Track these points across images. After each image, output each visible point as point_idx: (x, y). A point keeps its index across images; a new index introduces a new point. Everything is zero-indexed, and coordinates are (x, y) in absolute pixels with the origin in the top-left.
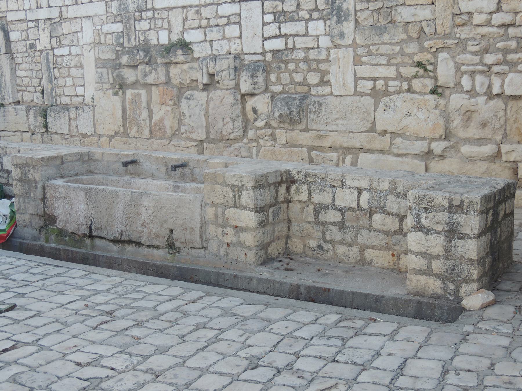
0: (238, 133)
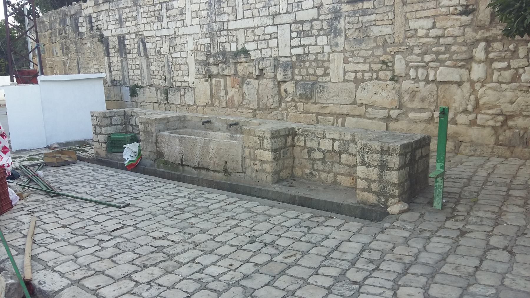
0: (276, 105)
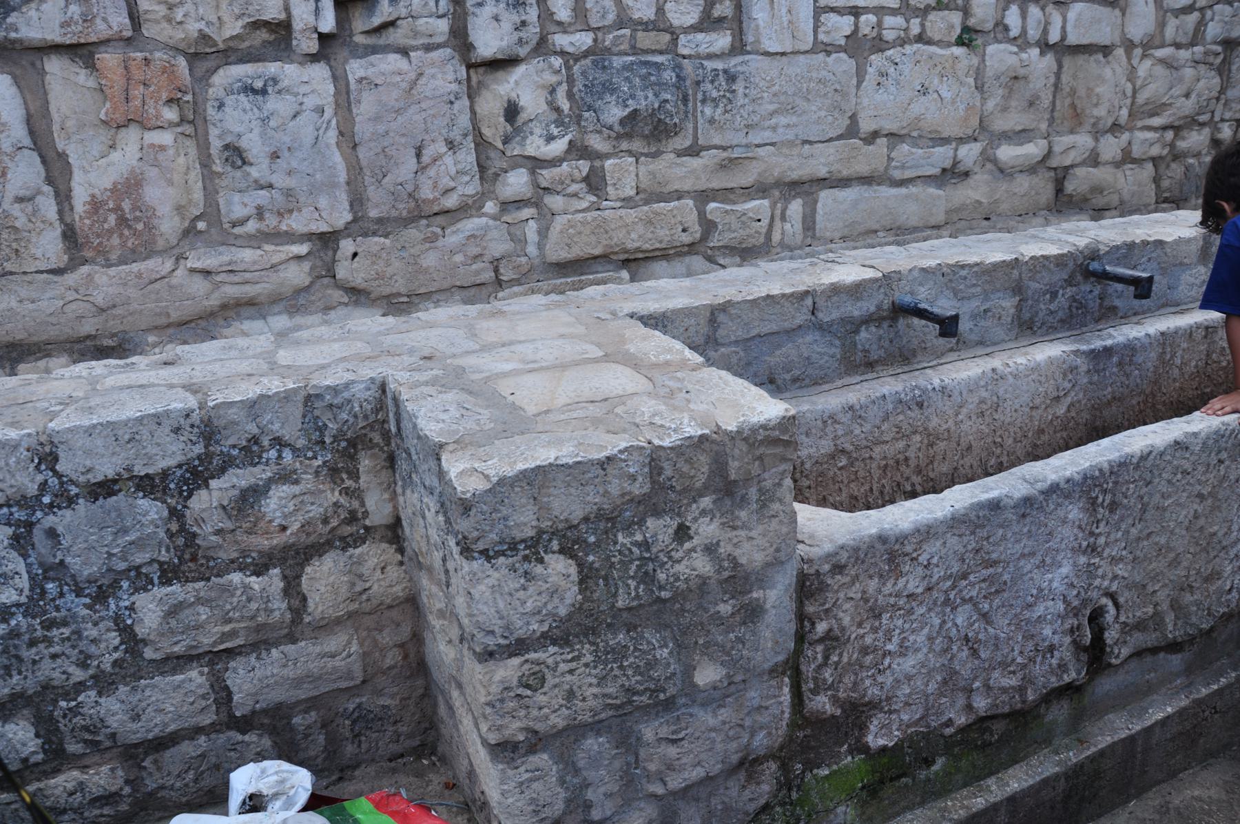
0: (472, 188)
